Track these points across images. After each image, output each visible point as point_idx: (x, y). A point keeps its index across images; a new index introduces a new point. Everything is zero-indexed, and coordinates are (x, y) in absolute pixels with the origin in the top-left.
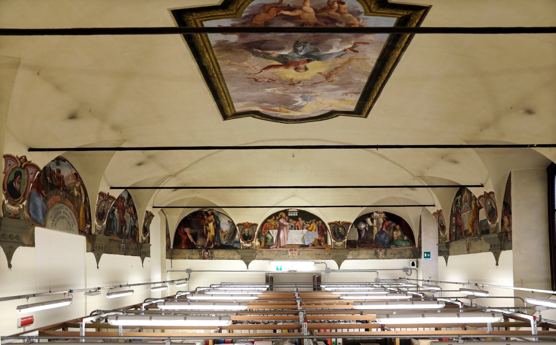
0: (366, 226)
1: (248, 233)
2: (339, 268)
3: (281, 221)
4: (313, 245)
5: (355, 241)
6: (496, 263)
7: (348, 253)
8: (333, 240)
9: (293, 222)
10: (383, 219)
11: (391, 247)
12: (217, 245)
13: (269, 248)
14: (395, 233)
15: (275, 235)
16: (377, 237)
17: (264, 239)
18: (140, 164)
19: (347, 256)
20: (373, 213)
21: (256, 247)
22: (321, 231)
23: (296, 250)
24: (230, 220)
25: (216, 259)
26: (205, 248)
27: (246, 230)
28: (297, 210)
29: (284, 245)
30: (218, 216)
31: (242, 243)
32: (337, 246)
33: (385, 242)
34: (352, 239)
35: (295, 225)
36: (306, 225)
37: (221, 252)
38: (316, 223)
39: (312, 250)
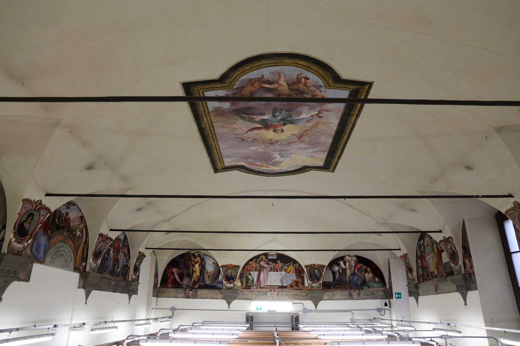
0: (339, 268)
1: (231, 274)
2: (316, 309)
3: (262, 263)
4: (291, 286)
5: (329, 283)
6: (464, 303)
7: (324, 294)
8: (309, 281)
9: (272, 264)
10: (355, 262)
11: (364, 288)
12: (201, 285)
13: (250, 289)
14: (366, 275)
16: (350, 279)
18: (139, 210)
19: (323, 297)
20: (345, 257)
21: (238, 287)
23: (275, 291)
24: (214, 261)
25: (199, 299)
26: (190, 288)
27: (229, 271)
28: (276, 254)
29: (264, 286)
30: (204, 258)
31: (225, 283)
32: (313, 287)
33: (357, 284)
34: (327, 280)
35: (274, 267)
36: (285, 267)
37: (205, 292)
39: (290, 291)
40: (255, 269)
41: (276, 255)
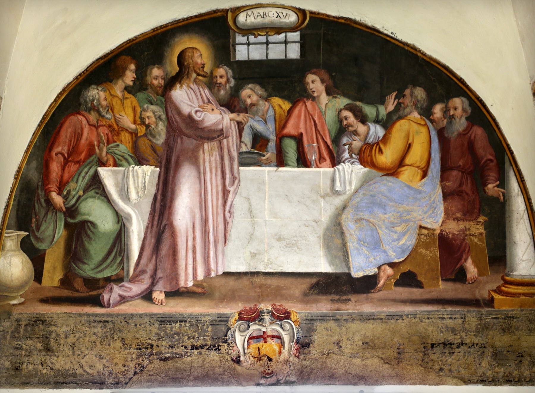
9: (263, 105)
13: (97, 302)
15: (136, 206)
17: (61, 233)
22: (462, 170)
23: (287, 315)
28: (293, 18)
29: (200, 276)
36: (361, 128)
38: (427, 113)
40: (135, 147)
41: (292, 29)
